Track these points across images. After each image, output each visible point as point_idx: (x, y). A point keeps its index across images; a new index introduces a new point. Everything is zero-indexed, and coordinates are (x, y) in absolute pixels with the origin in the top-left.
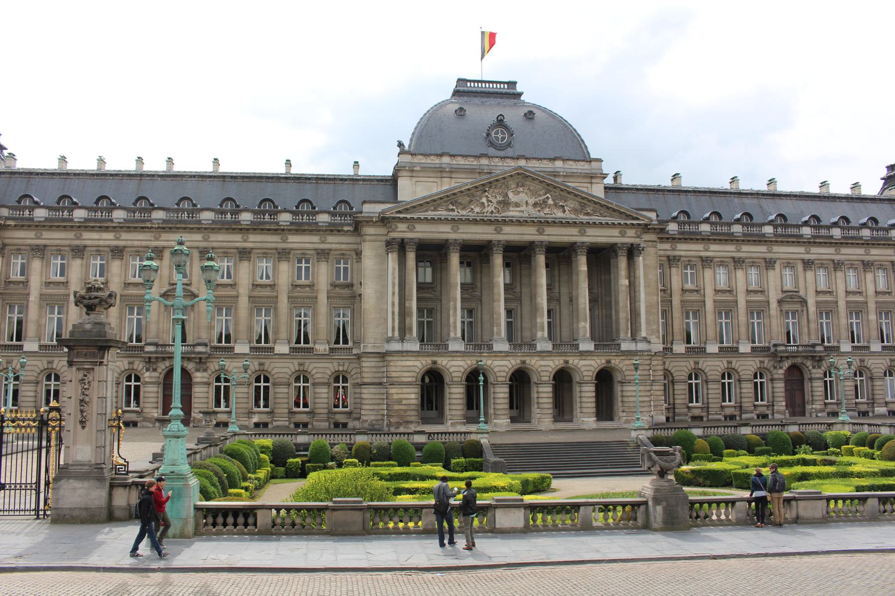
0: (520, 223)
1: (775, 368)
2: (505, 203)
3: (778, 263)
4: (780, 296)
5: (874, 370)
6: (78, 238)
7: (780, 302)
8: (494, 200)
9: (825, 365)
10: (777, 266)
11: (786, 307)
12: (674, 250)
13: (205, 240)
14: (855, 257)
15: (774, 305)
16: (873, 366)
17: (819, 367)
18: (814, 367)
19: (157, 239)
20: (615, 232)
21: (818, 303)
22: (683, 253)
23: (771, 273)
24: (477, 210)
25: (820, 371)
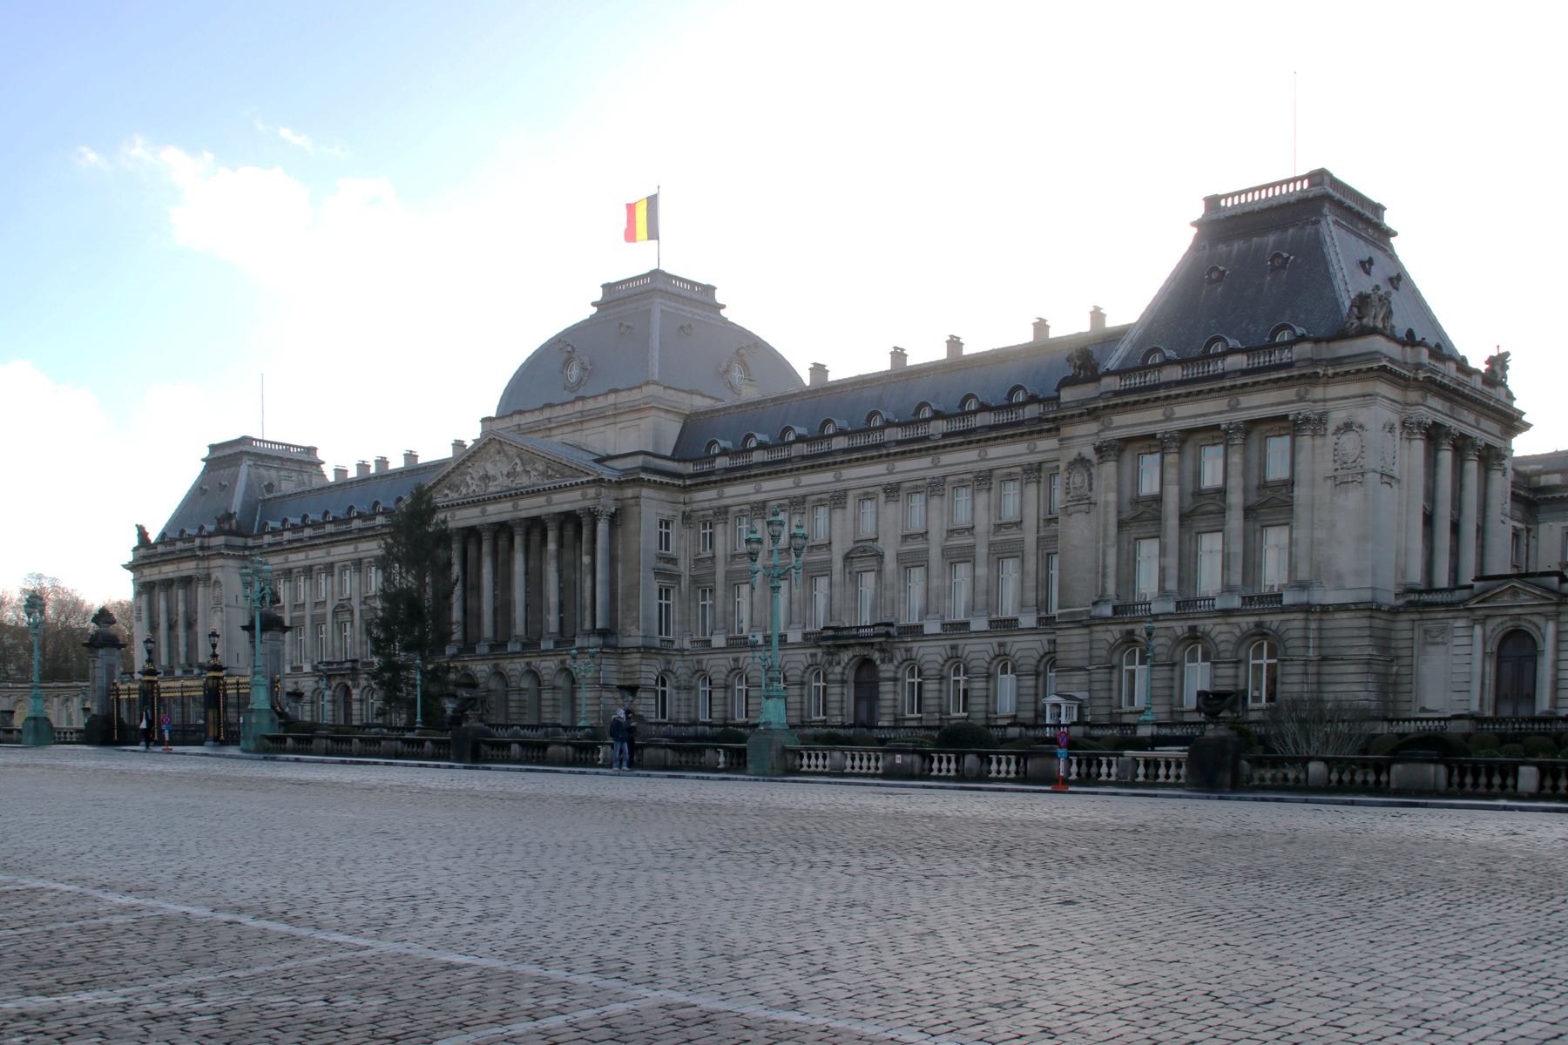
0: (496, 499)
1: (830, 664)
2: (486, 478)
3: (851, 494)
4: (851, 545)
5: (974, 663)
6: (287, 561)
7: (848, 558)
8: (476, 476)
9: (899, 656)
10: (850, 502)
11: (857, 565)
12: (720, 497)
13: (356, 551)
14: (961, 468)
15: (838, 565)
16: (972, 656)
17: (891, 661)
18: (883, 661)
19: (328, 554)
20: (577, 494)
21: (900, 557)
22: (729, 501)
23: (838, 514)
24: (464, 491)
25: (891, 667)
